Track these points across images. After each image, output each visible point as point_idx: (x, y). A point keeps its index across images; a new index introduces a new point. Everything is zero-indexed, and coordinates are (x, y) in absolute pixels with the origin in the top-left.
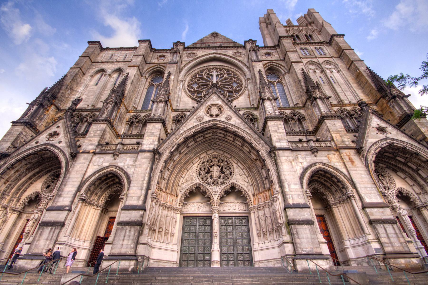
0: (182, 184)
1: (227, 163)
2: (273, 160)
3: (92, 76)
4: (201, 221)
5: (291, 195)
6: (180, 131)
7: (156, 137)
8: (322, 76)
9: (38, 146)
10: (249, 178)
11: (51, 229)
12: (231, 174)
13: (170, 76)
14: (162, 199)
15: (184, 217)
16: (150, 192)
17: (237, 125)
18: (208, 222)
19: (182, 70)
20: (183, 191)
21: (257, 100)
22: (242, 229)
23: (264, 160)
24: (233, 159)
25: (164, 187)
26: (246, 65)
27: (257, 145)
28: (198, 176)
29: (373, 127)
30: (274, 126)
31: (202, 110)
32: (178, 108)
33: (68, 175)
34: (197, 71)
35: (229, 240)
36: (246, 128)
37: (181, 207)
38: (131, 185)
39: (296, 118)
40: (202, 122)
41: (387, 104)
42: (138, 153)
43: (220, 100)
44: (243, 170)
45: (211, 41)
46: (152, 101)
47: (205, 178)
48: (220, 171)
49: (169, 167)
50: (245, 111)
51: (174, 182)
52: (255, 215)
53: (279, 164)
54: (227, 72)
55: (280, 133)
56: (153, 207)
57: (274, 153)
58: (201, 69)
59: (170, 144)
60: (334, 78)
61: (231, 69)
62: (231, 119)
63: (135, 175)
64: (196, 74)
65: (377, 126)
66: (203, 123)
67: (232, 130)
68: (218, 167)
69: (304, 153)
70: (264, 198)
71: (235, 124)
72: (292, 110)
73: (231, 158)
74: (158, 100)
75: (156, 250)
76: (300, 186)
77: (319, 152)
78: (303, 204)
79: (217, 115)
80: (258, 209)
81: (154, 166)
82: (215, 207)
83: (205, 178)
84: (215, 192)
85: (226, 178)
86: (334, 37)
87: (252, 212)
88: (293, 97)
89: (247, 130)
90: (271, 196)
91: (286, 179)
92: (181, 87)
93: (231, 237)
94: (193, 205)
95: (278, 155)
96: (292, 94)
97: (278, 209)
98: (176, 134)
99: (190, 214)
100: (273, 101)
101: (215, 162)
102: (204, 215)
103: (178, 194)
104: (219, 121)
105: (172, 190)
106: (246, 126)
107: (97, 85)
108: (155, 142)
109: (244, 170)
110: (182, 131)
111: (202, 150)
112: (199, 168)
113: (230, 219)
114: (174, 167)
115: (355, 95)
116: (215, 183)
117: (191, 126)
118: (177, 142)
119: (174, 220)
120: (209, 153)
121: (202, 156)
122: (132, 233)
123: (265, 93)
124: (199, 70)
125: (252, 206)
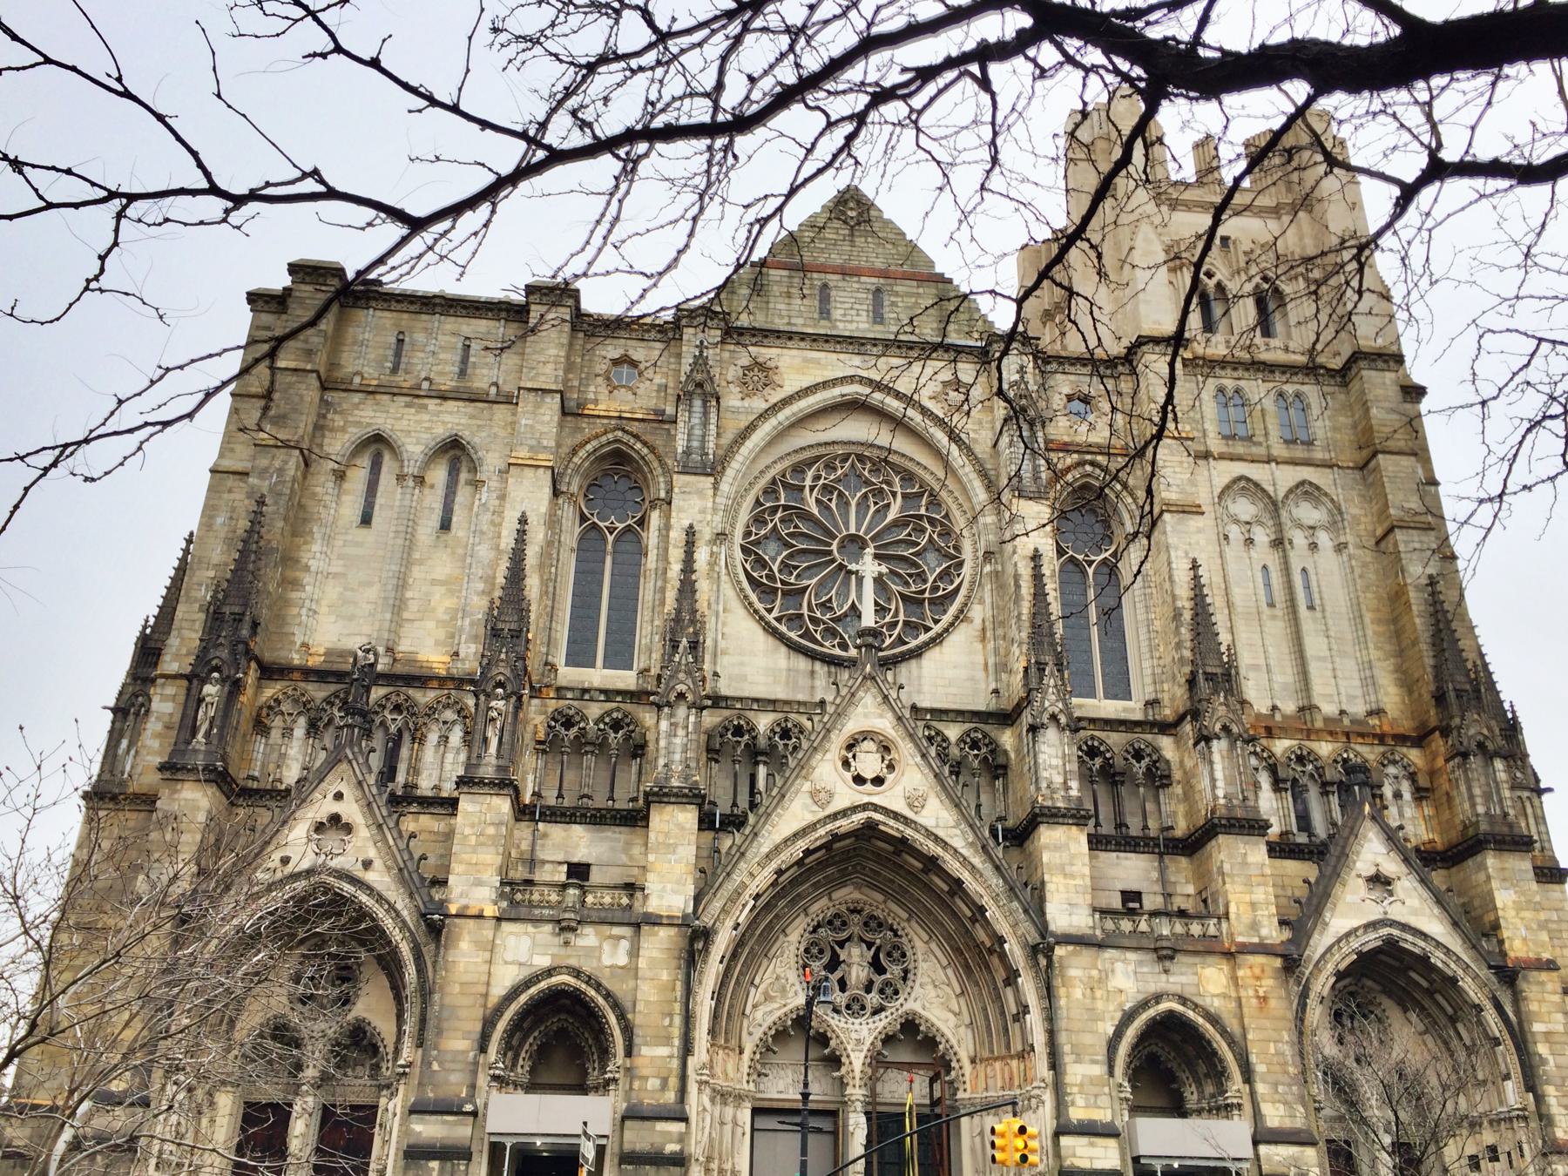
0: (754, 1006)
1: (896, 935)
3: (340, 476)
6: (761, 845)
8: (1271, 568)
9: (295, 877)
10: (962, 1001)
12: (905, 979)
16: (692, 1062)
17: (941, 833)
20: (758, 1033)
24: (913, 923)
26: (983, 474)
29: (1359, 876)
33: (436, 997)
34: (779, 467)
37: (752, 1086)
38: (637, 1040)
39: (1139, 768)
40: (830, 810)
41: (1447, 761)
42: (637, 926)
43: (890, 715)
44: (944, 968)
45: (836, 259)
50: (968, 726)
51: (731, 1006)
56: (705, 1109)
60: (1313, 578)
61: (921, 472)
63: (640, 1007)
64: (774, 482)
65: (1372, 871)
66: (834, 816)
67: (924, 849)
69: (1131, 956)
72: (1130, 736)
73: (908, 920)
74: (672, 698)
76: (1105, 1068)
77: (1179, 958)
78: (1104, 1125)
79: (878, 781)
82: (856, 1092)
84: (858, 1041)
85: (889, 991)
86: (1362, 364)
98: (749, 855)
101: (855, 929)
107: (366, 520)
109: (950, 972)
111: (816, 886)
115: (1369, 682)
116: (855, 1007)
117: (796, 826)
118: (753, 889)
119: (739, 1131)
120: (837, 895)
124: (787, 463)
125: (967, 1095)
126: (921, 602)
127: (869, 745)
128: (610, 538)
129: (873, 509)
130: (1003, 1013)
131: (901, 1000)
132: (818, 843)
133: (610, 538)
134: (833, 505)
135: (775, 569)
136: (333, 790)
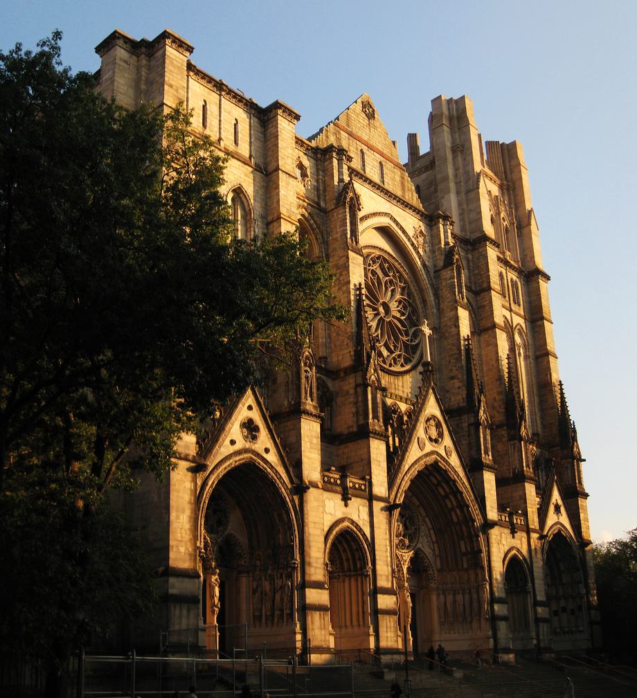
10: (436, 545)
11: (320, 615)
40: (425, 451)
41: (561, 459)
44: (429, 530)
109: (432, 531)
110: (407, 467)
117: (415, 458)
122: (392, 624)
127: (432, 422)
136: (247, 405)
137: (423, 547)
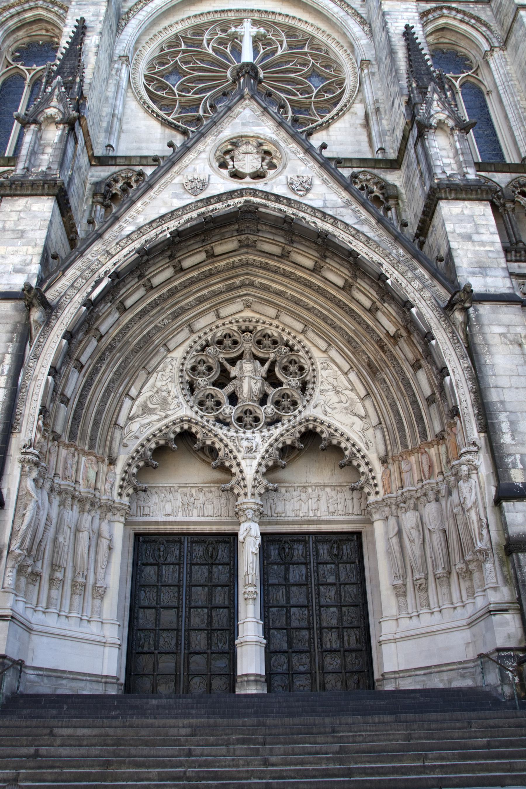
0: (130, 419)
2: (461, 335)
4: (199, 550)
5: (518, 456)
6: (122, 229)
7: (36, 245)
10: (368, 403)
12: (304, 388)
13: (84, 34)
14: (60, 472)
15: (137, 536)
17: (330, 213)
18: (222, 553)
19: (128, 20)
20: (134, 445)
21: (399, 134)
22: (338, 576)
23: (428, 336)
24: (310, 334)
25: (64, 430)
27: (404, 283)
28: (189, 393)
30: (460, 219)
31: (203, 156)
32: (111, 154)
34: (180, 27)
35: (293, 610)
36: (361, 222)
37: (126, 500)
40: (203, 196)
46: (18, 118)
47: (210, 403)
48: (266, 379)
49: (83, 359)
51: (99, 413)
52: (387, 526)
53: (481, 349)
54: (288, 36)
55: (483, 243)
56: (28, 493)
57: (465, 310)
58: (194, 22)
59: (87, 273)
61: (303, 27)
62: (308, 190)
66: (208, 201)
68: (257, 363)
70: (422, 471)
71: (325, 206)
72: (514, 175)
75: (45, 640)
79: (258, 176)
80: (398, 506)
81: (29, 352)
83: (210, 403)
84: (250, 450)
85: (286, 403)
87: (376, 517)
88: (516, 133)
89: (365, 229)
90: (448, 462)
91: (502, 402)
92: (124, 83)
93: (303, 600)
94: (170, 497)
95: (478, 317)
96: (513, 123)
97: (475, 503)
98: (106, 236)
99: (157, 523)
100: (457, 132)
102: (207, 529)
103: (114, 455)
104: (267, 195)
105: (93, 439)
106: (364, 214)
108: (30, 263)
109: (352, 376)
110: (129, 229)
111: (200, 301)
112: (188, 365)
113: (298, 541)
114: (101, 360)
117: (164, 211)
118: (109, 266)
119: (104, 543)
120: (225, 311)
121: (201, 323)
123: (429, 104)
124: (187, 24)
125: (379, 497)
126: (307, 110)
128: (29, 77)
129: (262, 51)
130: (414, 402)
131: (300, 408)
132: (189, 225)
133: (29, 77)
134: (228, 51)
135: (175, 89)
137: (325, 413)
